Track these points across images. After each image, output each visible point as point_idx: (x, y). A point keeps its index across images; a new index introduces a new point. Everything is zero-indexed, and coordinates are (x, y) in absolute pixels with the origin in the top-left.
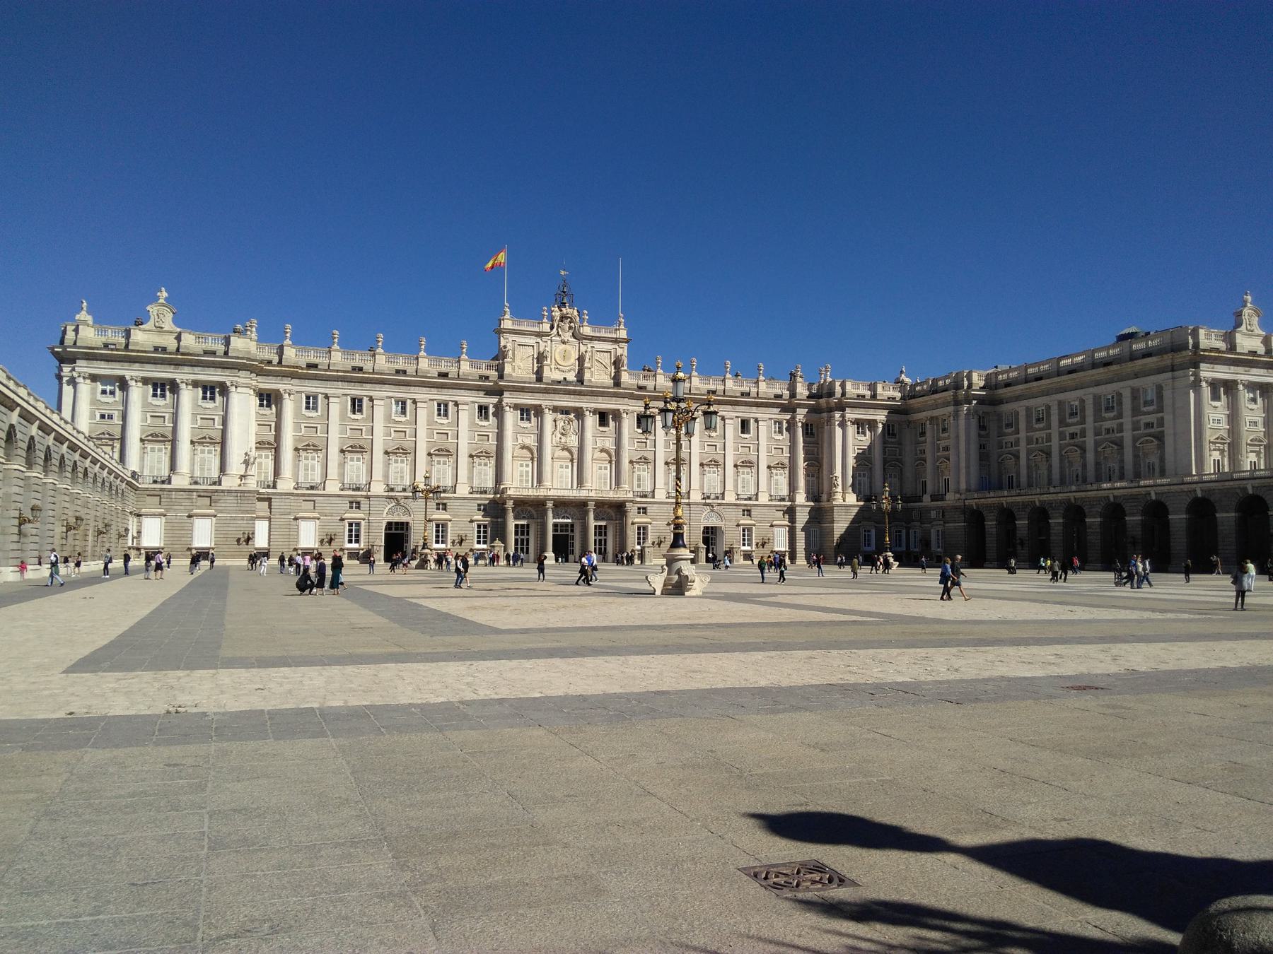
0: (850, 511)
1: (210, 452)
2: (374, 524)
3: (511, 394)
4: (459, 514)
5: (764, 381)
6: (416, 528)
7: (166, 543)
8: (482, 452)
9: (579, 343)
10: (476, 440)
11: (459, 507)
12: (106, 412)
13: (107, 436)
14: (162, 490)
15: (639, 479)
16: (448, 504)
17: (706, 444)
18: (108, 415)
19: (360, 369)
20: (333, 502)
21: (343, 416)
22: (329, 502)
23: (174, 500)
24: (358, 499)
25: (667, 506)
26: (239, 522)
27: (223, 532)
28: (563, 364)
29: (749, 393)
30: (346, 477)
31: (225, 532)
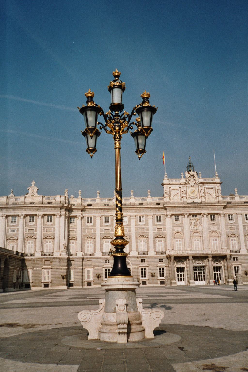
1: (50, 242)
3: (170, 210)
4: (151, 264)
7: (33, 280)
8: (159, 236)
10: (156, 230)
12: (13, 229)
13: (13, 238)
14: (32, 259)
15: (233, 244)
16: (146, 260)
18: (14, 230)
19: (108, 205)
21: (101, 225)
23: (36, 262)
24: (109, 259)
26: (61, 270)
27: (54, 275)
28: (193, 195)
31: (55, 275)
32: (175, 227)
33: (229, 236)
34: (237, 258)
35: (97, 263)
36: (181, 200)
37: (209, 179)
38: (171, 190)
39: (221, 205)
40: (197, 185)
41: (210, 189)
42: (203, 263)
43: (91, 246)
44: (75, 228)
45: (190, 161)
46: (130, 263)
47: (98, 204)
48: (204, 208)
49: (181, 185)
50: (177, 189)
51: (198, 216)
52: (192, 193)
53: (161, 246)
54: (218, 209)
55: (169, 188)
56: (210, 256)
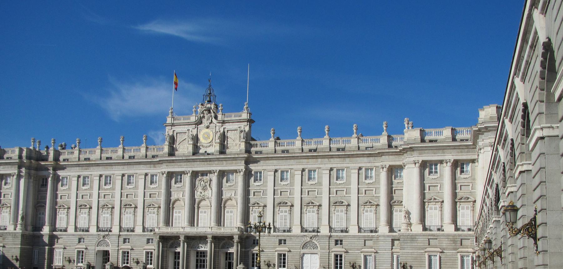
0: (416, 239)
2: (90, 252)
3: (167, 166)
4: (136, 245)
5: (356, 137)
6: (113, 254)
9: (216, 127)
11: (136, 241)
16: (130, 239)
20: (71, 239)
22: (70, 239)
24: (83, 237)
25: (274, 238)
26: (14, 250)
28: (206, 142)
29: (345, 148)
30: (79, 224)
32: (174, 191)
35: (68, 242)
37: (233, 114)
39: (240, 156)
41: (232, 130)
42: (206, 247)
43: (63, 218)
44: (46, 193)
45: (210, 86)
47: (75, 157)
48: (216, 162)
49: (189, 126)
50: (185, 132)
51: (208, 174)
52: (205, 138)
54: (237, 164)
56: (209, 236)
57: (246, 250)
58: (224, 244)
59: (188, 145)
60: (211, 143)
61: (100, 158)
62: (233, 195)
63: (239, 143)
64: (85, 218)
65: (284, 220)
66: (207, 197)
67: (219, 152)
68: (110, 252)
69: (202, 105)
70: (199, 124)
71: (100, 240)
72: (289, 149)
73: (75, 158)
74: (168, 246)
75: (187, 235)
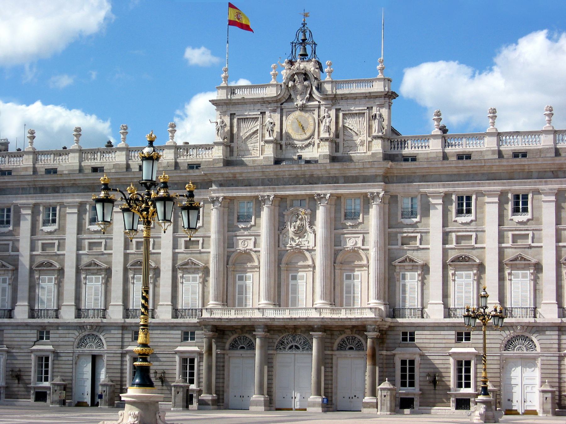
2: (64, 358)
3: (221, 185)
4: (159, 344)
6: (111, 363)
9: (319, 108)
17: (510, 234)
19: (55, 171)
24: (48, 328)
33: (395, 266)
34: (412, 334)
35: (16, 339)
36: (262, 151)
38: (235, 120)
40: (317, 103)
45: (304, 25)
46: (104, 341)
47: (27, 168)
53: (194, 293)
55: (231, 114)
57: (389, 353)
58: (344, 341)
59: (262, 143)
60: (310, 140)
61: (78, 168)
62: (360, 244)
63: (369, 139)
64: (49, 292)
65: (466, 292)
66: (306, 248)
67: (328, 157)
68: (105, 358)
69: (291, 63)
70: (285, 100)
71: (84, 334)
72: (472, 152)
73: (26, 169)
74: (227, 346)
75: (270, 323)
